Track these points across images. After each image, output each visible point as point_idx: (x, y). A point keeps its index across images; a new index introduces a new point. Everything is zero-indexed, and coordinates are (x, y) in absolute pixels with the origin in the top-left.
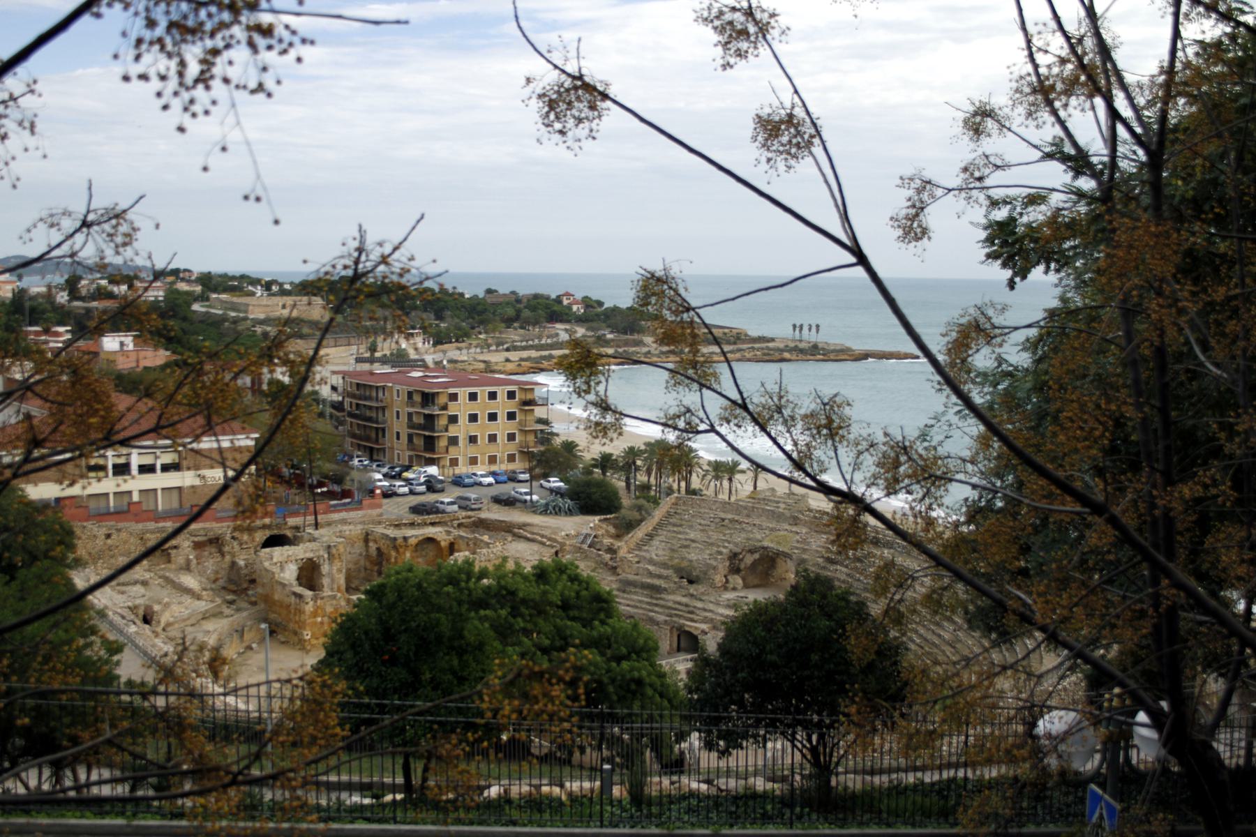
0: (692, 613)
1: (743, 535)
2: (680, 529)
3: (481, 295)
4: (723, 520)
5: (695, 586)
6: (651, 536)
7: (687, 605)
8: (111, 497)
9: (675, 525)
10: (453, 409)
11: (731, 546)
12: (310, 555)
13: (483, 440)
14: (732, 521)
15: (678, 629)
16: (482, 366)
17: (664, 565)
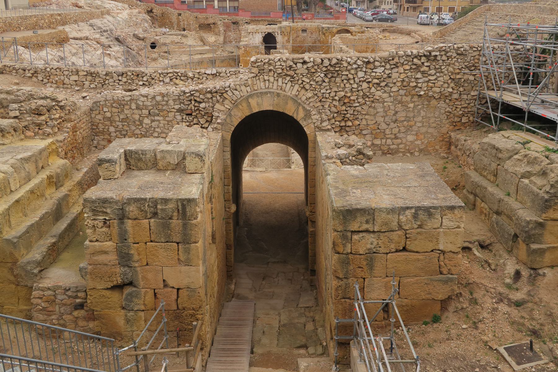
12: (270, 31)
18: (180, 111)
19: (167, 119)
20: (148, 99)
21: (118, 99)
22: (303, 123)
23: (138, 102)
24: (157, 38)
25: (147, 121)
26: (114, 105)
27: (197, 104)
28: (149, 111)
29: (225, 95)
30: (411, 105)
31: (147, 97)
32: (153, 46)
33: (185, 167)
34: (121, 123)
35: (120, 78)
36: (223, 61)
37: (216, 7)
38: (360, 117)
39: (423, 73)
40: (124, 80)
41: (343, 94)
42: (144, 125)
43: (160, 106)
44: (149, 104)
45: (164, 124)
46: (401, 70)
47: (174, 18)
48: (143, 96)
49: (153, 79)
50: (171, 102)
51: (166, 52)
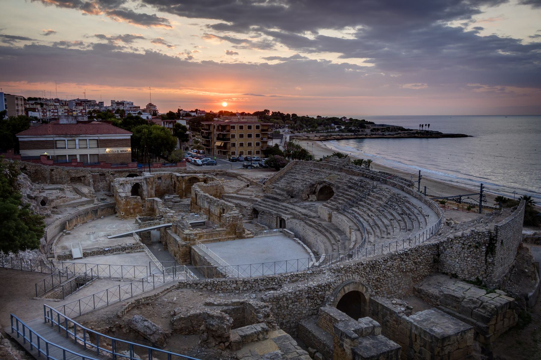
0: (286, 210)
1: (318, 177)
2: (294, 174)
3: (315, 118)
5: (293, 199)
8: (67, 156)
9: (292, 173)
10: (232, 132)
12: (138, 182)
13: (245, 145)
14: (315, 171)
15: (280, 218)
16: (306, 138)
17: (283, 190)
18: (308, 298)
22: (365, 294)
24: (44, 194)
25: (291, 306)
30: (400, 276)
32: (43, 203)
33: (374, 332)
36: (102, 210)
37: (78, 160)
39: (404, 261)
41: (377, 276)
46: (397, 261)
47: (47, 174)
48: (289, 293)
50: (304, 294)
51: (54, 208)
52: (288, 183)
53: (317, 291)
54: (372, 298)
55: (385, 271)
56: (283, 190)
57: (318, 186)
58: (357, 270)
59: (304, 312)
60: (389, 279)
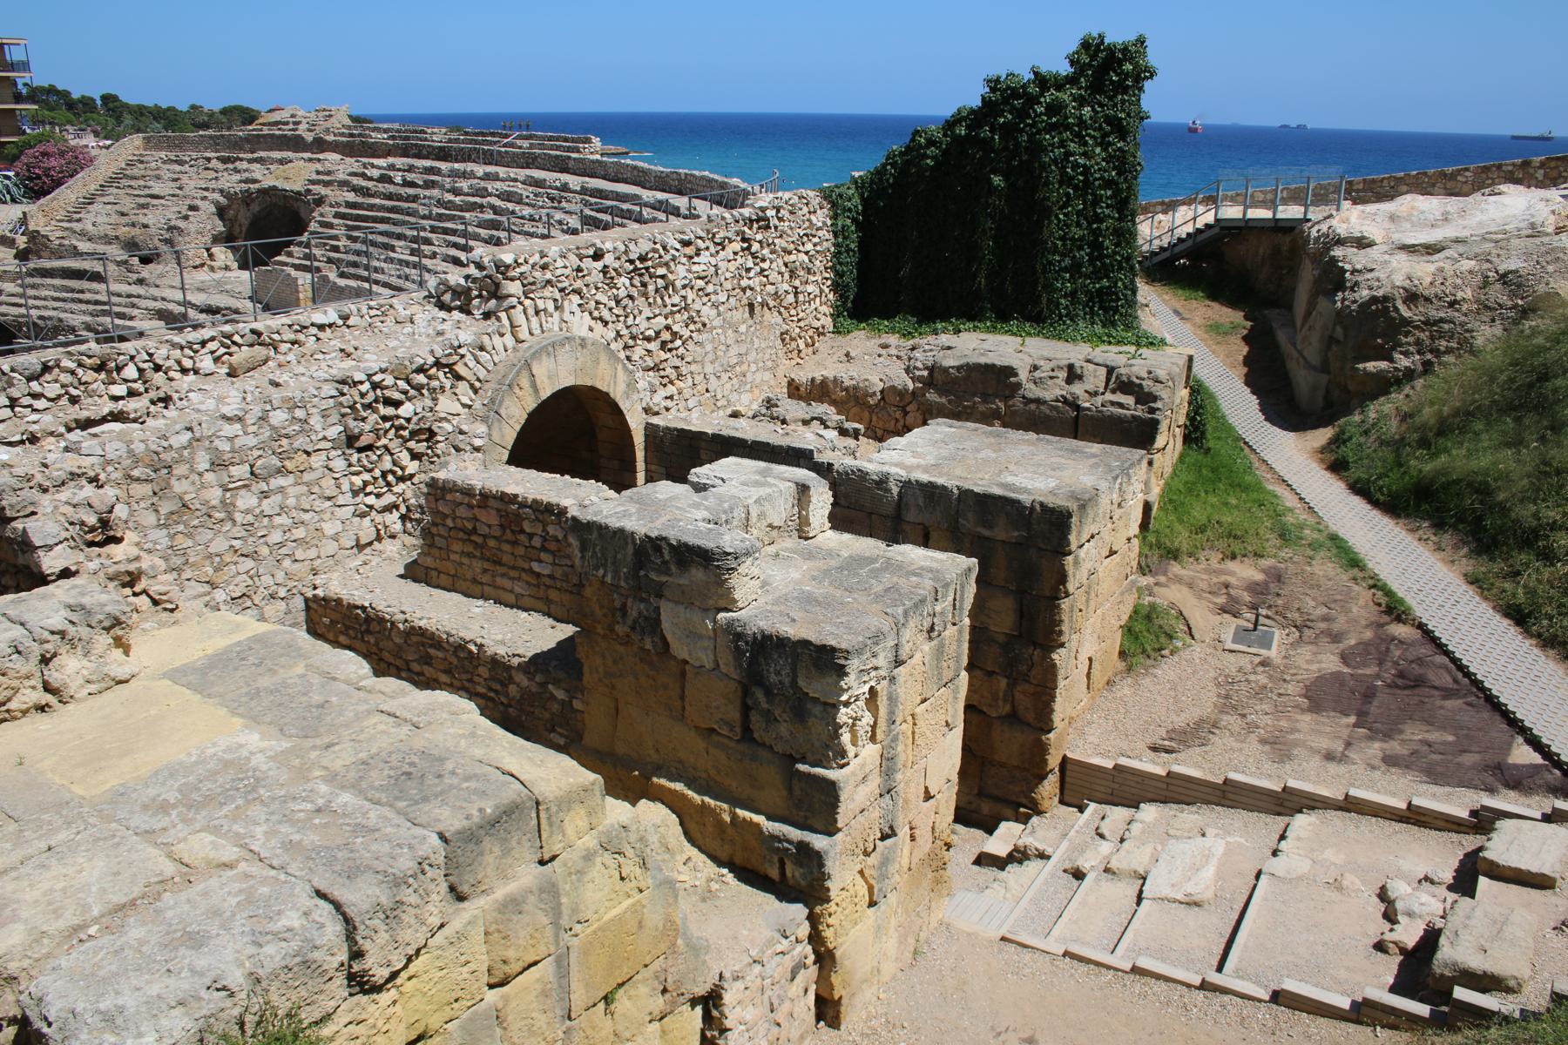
2: (142, 183)
4: (209, 160)
6: (91, 200)
7: (129, 296)
11: (217, 196)
19: (307, 477)
20: (244, 426)
21: (147, 449)
22: (624, 406)
23: (217, 443)
25: (246, 500)
26: (136, 473)
27: (390, 411)
28: (252, 466)
29: (460, 368)
31: (240, 419)
34: (165, 532)
35: (35, 386)
38: (684, 370)
40: (53, 390)
41: (660, 321)
42: (238, 517)
43: (285, 442)
44: (251, 441)
45: (298, 498)
49: (158, 368)
52: (123, 214)
53: (389, 402)
54: (655, 420)
55: (691, 295)
56: (108, 240)
57: (243, 210)
58: (579, 284)
59: (330, 528)
60: (704, 337)
